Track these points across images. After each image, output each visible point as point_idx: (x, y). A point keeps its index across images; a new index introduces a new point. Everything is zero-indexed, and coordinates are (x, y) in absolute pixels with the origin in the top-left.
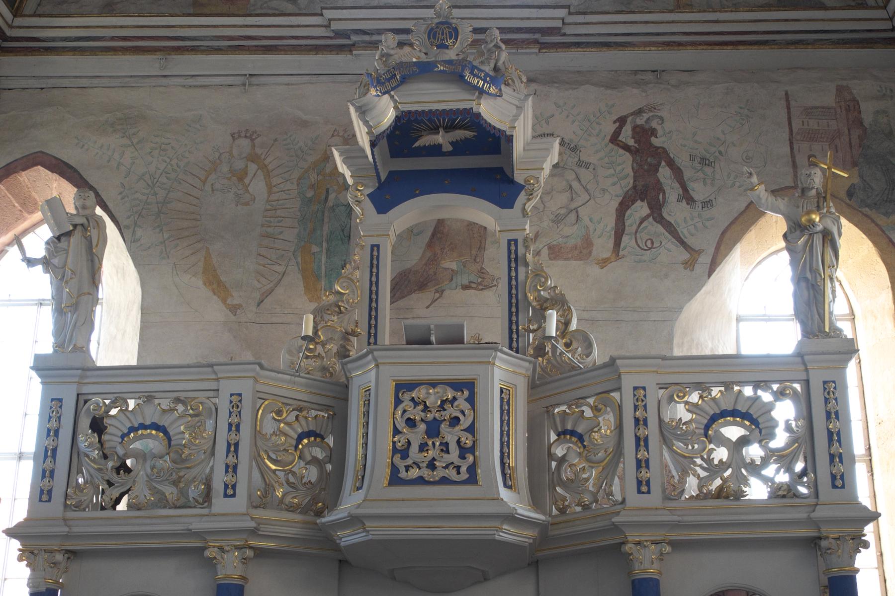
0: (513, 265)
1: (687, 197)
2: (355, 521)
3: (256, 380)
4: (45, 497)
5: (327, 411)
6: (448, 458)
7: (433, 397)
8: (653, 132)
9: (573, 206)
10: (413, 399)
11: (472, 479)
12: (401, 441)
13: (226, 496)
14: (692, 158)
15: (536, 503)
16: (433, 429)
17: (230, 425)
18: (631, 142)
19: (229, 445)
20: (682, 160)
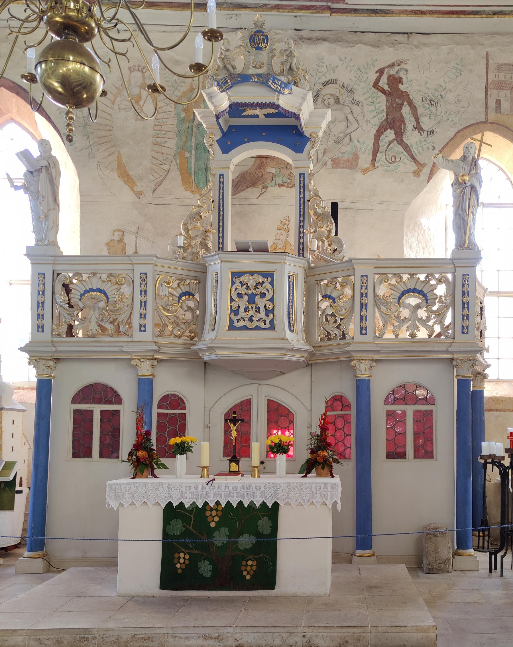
1: (418, 127)
18: (386, 87)
20: (417, 101)
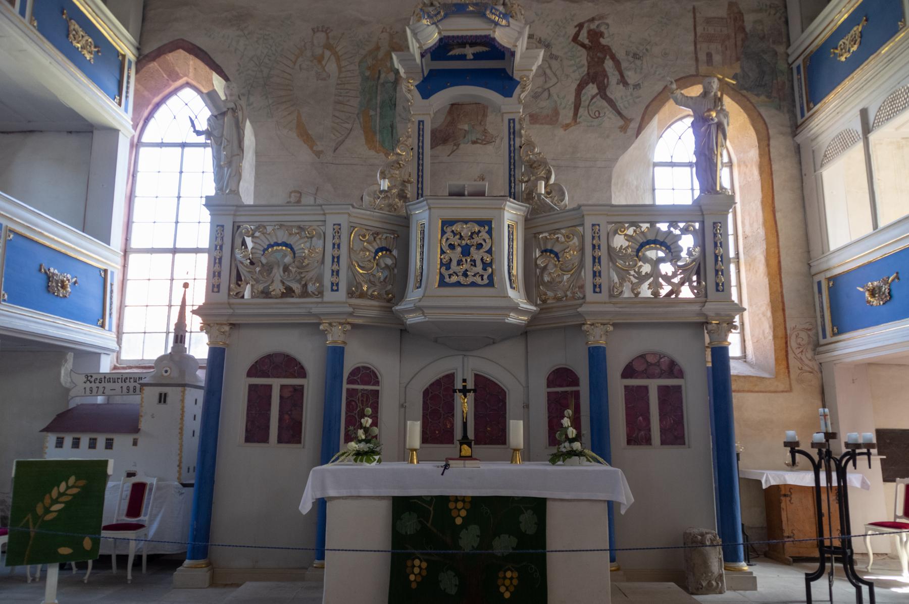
0: (512, 136)
1: (623, 81)
2: (418, 309)
3: (349, 215)
4: (216, 290)
5: (393, 234)
6: (475, 270)
7: (465, 230)
8: (601, 35)
9: (546, 86)
10: (453, 231)
11: (491, 284)
12: (446, 259)
13: (332, 290)
14: (627, 54)
15: (529, 298)
16: (466, 251)
17: (334, 244)
18: (586, 42)
19: (333, 258)
20: (621, 55)
